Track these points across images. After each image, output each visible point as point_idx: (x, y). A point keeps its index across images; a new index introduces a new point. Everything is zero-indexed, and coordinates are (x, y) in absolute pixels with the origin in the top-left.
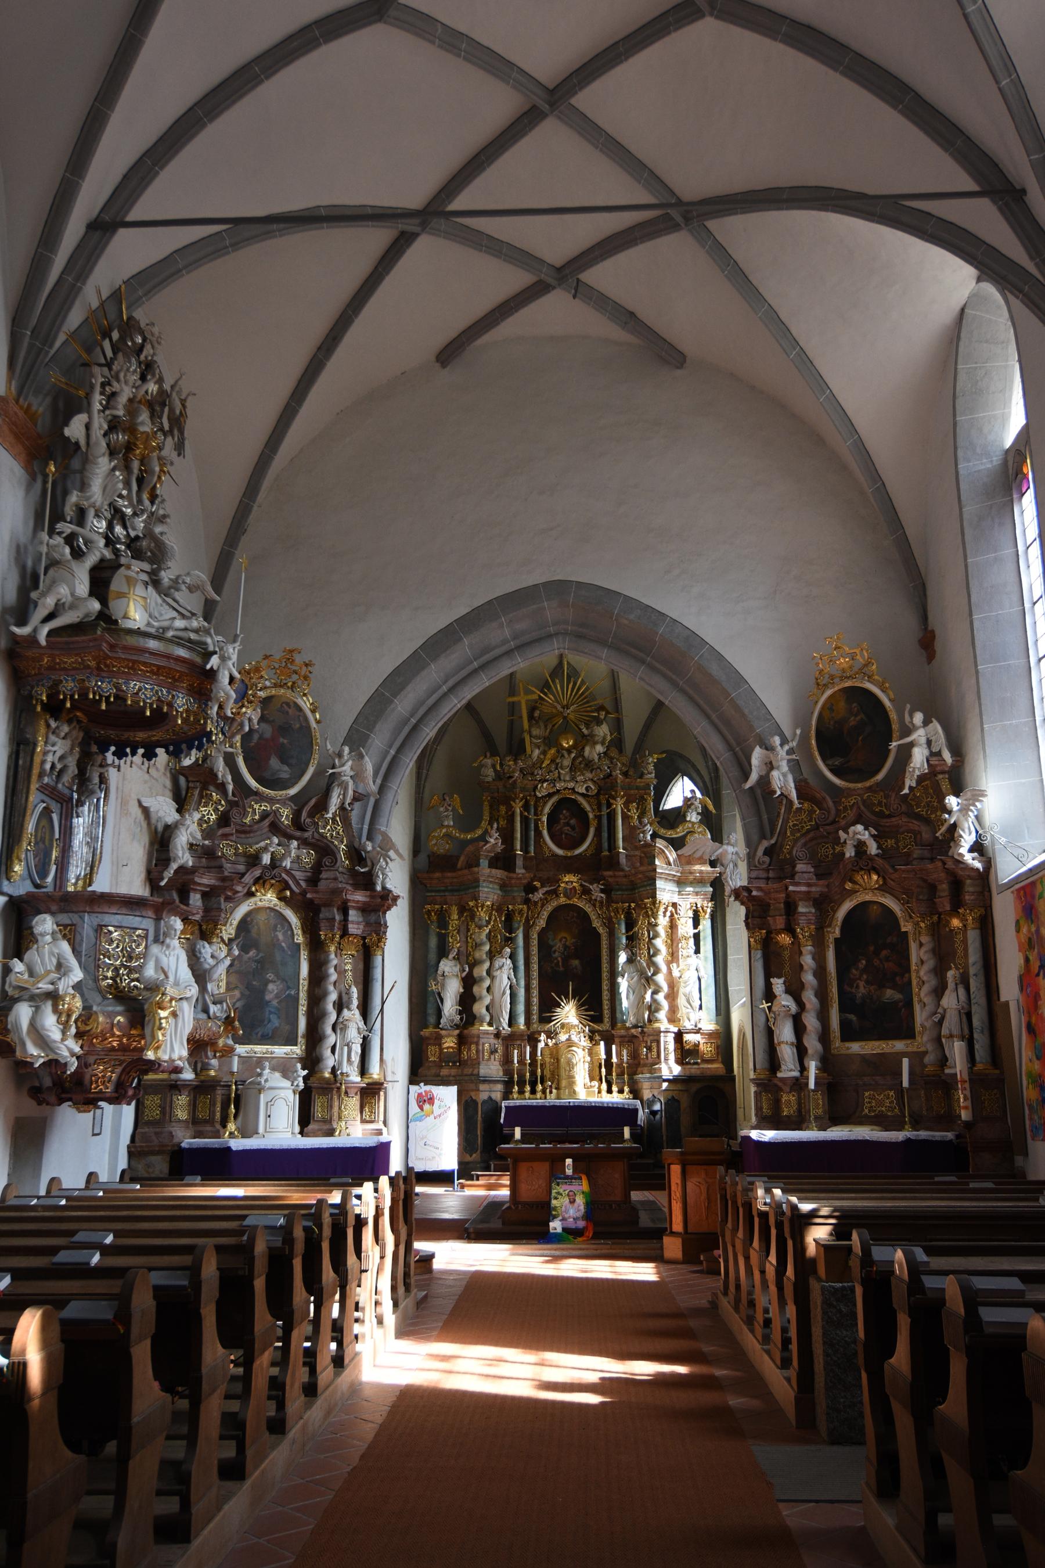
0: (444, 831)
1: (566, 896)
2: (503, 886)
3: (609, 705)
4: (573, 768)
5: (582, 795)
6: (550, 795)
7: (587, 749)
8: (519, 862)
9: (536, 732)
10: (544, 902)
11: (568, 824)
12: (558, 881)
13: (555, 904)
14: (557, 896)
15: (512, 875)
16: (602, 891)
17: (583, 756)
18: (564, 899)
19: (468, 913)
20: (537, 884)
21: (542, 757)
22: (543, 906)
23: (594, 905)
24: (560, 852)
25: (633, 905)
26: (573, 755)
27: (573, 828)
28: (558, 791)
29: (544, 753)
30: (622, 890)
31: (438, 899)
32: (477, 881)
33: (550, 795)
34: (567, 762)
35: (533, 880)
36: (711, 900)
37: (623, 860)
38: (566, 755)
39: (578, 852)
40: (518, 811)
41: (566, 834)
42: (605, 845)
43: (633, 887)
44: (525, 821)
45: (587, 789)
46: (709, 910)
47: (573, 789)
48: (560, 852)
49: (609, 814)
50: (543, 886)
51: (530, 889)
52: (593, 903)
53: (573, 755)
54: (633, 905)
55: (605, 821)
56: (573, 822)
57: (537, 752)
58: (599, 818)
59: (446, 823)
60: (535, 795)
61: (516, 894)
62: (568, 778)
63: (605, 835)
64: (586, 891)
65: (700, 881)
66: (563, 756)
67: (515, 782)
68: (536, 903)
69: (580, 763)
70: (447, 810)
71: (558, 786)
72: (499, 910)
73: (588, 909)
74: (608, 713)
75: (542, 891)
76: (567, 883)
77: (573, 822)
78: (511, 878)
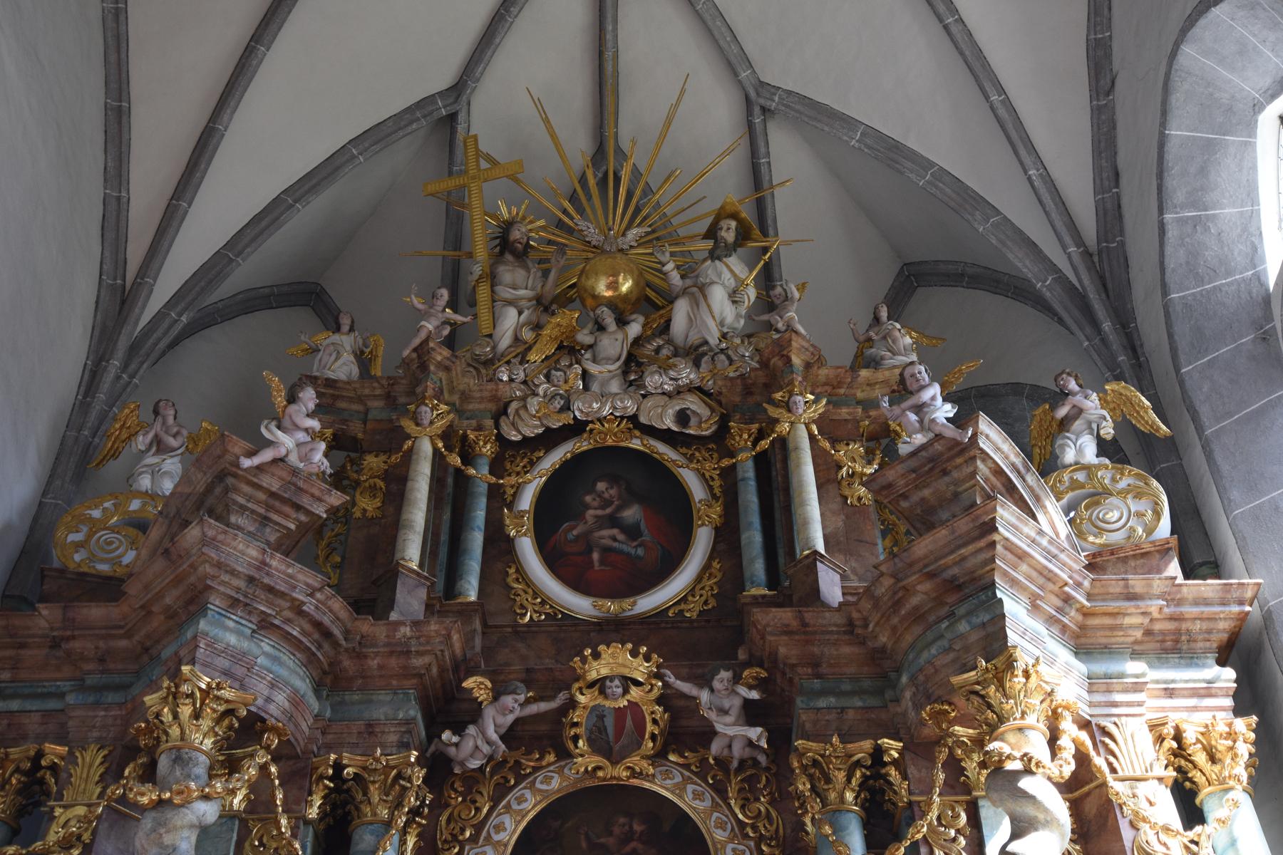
0: (135, 505)
1: (600, 745)
2: (329, 681)
3: (747, 213)
4: (633, 364)
5: (666, 436)
6: (550, 439)
7: (681, 310)
8: (410, 601)
9: (510, 274)
10: (503, 776)
11: (613, 521)
12: (565, 681)
13: (553, 783)
14: (565, 755)
15: (366, 626)
16: (751, 713)
17: (669, 342)
18: (592, 761)
19: (137, 753)
20: (477, 685)
21: (527, 335)
22: (502, 791)
23: (720, 790)
24: (581, 605)
25: (893, 747)
26: (634, 329)
27: (632, 532)
28: (577, 428)
29: (537, 327)
30: (840, 694)
31: (32, 724)
32: (195, 603)
33: (550, 439)
34: (614, 344)
35: (464, 667)
36: (1238, 711)
37: (831, 586)
38: (609, 320)
39: (648, 602)
40: (426, 448)
41: (606, 550)
42: (758, 568)
43: (882, 670)
44: (451, 494)
45: (683, 417)
46: (1244, 750)
47: (634, 419)
48: (581, 605)
49: (762, 461)
50: (496, 696)
51: (447, 709)
52: (717, 776)
53: (634, 329)
54: (893, 747)
55: (750, 497)
56: (632, 513)
57: (510, 319)
58: (729, 494)
59: (145, 482)
60: (497, 426)
61: (379, 713)
62: (615, 387)
63: (753, 538)
64: (685, 733)
65: (1171, 645)
66: (601, 328)
67: (422, 350)
68: (472, 780)
69: (657, 351)
70: (160, 446)
71: (580, 409)
72: (296, 766)
73: (693, 801)
74: (744, 235)
75: (494, 721)
76: (600, 685)
77: (632, 513)
78: (364, 640)
